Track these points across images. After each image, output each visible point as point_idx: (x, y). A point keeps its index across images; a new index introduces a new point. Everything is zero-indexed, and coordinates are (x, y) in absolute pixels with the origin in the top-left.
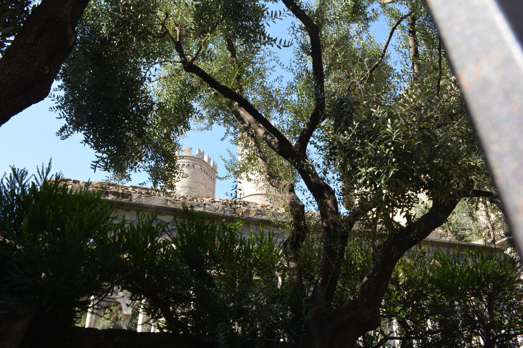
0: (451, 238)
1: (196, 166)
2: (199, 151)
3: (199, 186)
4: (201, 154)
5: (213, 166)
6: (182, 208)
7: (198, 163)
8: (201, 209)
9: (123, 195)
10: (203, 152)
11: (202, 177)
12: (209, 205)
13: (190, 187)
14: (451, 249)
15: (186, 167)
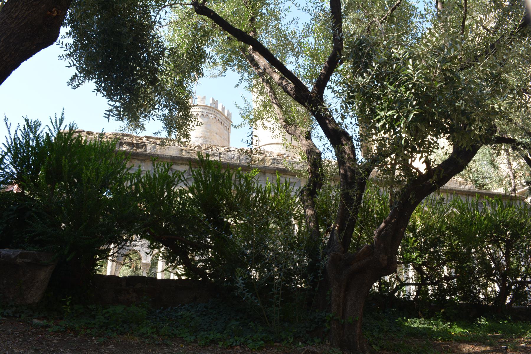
0: (470, 186)
1: (210, 115)
2: (213, 99)
3: (214, 135)
4: (215, 102)
5: (228, 115)
6: (197, 157)
7: (212, 112)
8: (217, 158)
9: (138, 146)
10: (217, 101)
11: (217, 127)
12: (224, 154)
13: (205, 138)
14: (470, 198)
15: (200, 117)
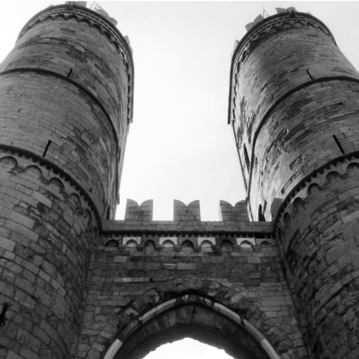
1: (122, 50)
